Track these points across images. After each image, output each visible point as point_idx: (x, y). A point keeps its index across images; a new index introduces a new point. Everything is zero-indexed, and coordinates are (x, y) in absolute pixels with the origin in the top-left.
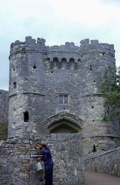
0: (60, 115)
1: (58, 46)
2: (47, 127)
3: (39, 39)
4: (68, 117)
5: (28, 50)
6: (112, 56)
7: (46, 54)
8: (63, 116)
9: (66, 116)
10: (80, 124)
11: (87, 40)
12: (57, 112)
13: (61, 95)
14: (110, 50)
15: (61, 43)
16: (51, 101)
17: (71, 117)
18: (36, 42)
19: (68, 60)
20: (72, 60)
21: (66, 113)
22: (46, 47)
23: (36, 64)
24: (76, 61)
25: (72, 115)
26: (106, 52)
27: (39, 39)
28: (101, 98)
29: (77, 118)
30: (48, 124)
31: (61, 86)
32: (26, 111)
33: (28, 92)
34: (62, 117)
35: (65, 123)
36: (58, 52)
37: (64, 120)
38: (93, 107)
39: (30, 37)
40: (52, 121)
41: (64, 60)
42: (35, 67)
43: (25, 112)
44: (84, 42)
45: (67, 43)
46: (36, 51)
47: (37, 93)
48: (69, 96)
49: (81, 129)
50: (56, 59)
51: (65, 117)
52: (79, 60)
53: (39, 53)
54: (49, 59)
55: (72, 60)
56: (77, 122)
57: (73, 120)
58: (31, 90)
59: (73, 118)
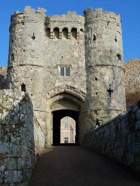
4: (68, 90)
6: (117, 25)
12: (57, 85)
14: (115, 19)
16: (51, 73)
20: (74, 30)
21: (67, 86)
23: (35, 34)
24: (78, 30)
25: (74, 88)
26: (111, 21)
29: (79, 91)
31: (62, 57)
32: (23, 83)
34: (63, 90)
35: (67, 96)
37: (65, 93)
38: (96, 79)
41: (65, 30)
47: (35, 63)
50: (56, 30)
51: (67, 89)
53: (39, 22)
55: (74, 30)
56: (79, 94)
57: (75, 92)
59: (74, 91)
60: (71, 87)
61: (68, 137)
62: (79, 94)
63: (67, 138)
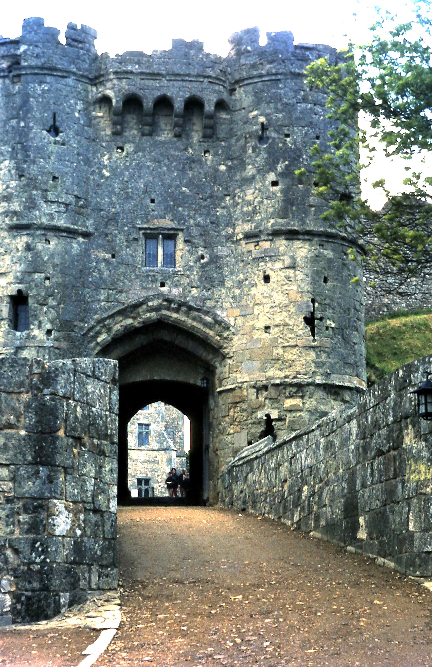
0: (144, 307)
1: (141, 54)
2: (99, 348)
3: (72, 27)
5: (31, 67)
7: (96, 80)
8: (157, 309)
9: (168, 309)
10: (218, 338)
11: (252, 34)
13: (151, 236)
15: (154, 41)
16: (113, 256)
17: (187, 314)
18: (62, 40)
19: (179, 105)
20: (194, 104)
22: (96, 58)
23: (58, 119)
24: (209, 108)
27: (72, 27)
28: (297, 244)
30: (99, 340)
31: (153, 201)
32: (19, 291)
33: (25, 222)
34: (153, 315)
36: (142, 73)
37: (161, 324)
39: (39, 22)
40: (118, 327)
41: (164, 103)
42: (54, 130)
43: (14, 293)
44: (243, 42)
45: (179, 45)
46: (60, 70)
47: (62, 223)
48: (181, 237)
49: (224, 357)
51: (164, 312)
52: (221, 105)
54: (106, 100)
55: (194, 104)
56: (208, 331)
57: (195, 324)
58: (44, 214)
59: (194, 319)
60: (181, 305)
61: (150, 475)
62: (208, 331)
63: (147, 481)
